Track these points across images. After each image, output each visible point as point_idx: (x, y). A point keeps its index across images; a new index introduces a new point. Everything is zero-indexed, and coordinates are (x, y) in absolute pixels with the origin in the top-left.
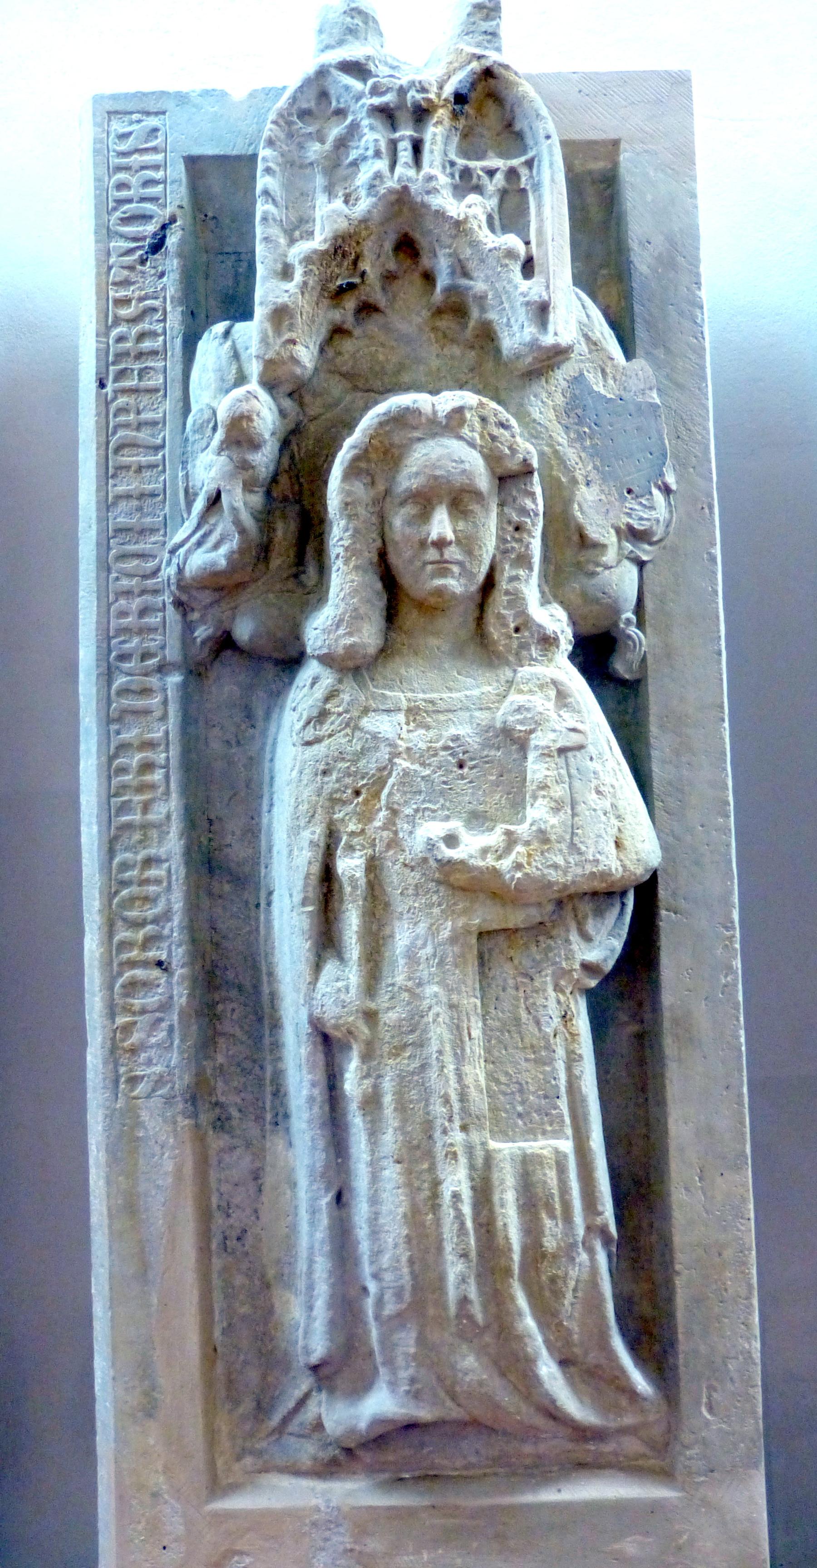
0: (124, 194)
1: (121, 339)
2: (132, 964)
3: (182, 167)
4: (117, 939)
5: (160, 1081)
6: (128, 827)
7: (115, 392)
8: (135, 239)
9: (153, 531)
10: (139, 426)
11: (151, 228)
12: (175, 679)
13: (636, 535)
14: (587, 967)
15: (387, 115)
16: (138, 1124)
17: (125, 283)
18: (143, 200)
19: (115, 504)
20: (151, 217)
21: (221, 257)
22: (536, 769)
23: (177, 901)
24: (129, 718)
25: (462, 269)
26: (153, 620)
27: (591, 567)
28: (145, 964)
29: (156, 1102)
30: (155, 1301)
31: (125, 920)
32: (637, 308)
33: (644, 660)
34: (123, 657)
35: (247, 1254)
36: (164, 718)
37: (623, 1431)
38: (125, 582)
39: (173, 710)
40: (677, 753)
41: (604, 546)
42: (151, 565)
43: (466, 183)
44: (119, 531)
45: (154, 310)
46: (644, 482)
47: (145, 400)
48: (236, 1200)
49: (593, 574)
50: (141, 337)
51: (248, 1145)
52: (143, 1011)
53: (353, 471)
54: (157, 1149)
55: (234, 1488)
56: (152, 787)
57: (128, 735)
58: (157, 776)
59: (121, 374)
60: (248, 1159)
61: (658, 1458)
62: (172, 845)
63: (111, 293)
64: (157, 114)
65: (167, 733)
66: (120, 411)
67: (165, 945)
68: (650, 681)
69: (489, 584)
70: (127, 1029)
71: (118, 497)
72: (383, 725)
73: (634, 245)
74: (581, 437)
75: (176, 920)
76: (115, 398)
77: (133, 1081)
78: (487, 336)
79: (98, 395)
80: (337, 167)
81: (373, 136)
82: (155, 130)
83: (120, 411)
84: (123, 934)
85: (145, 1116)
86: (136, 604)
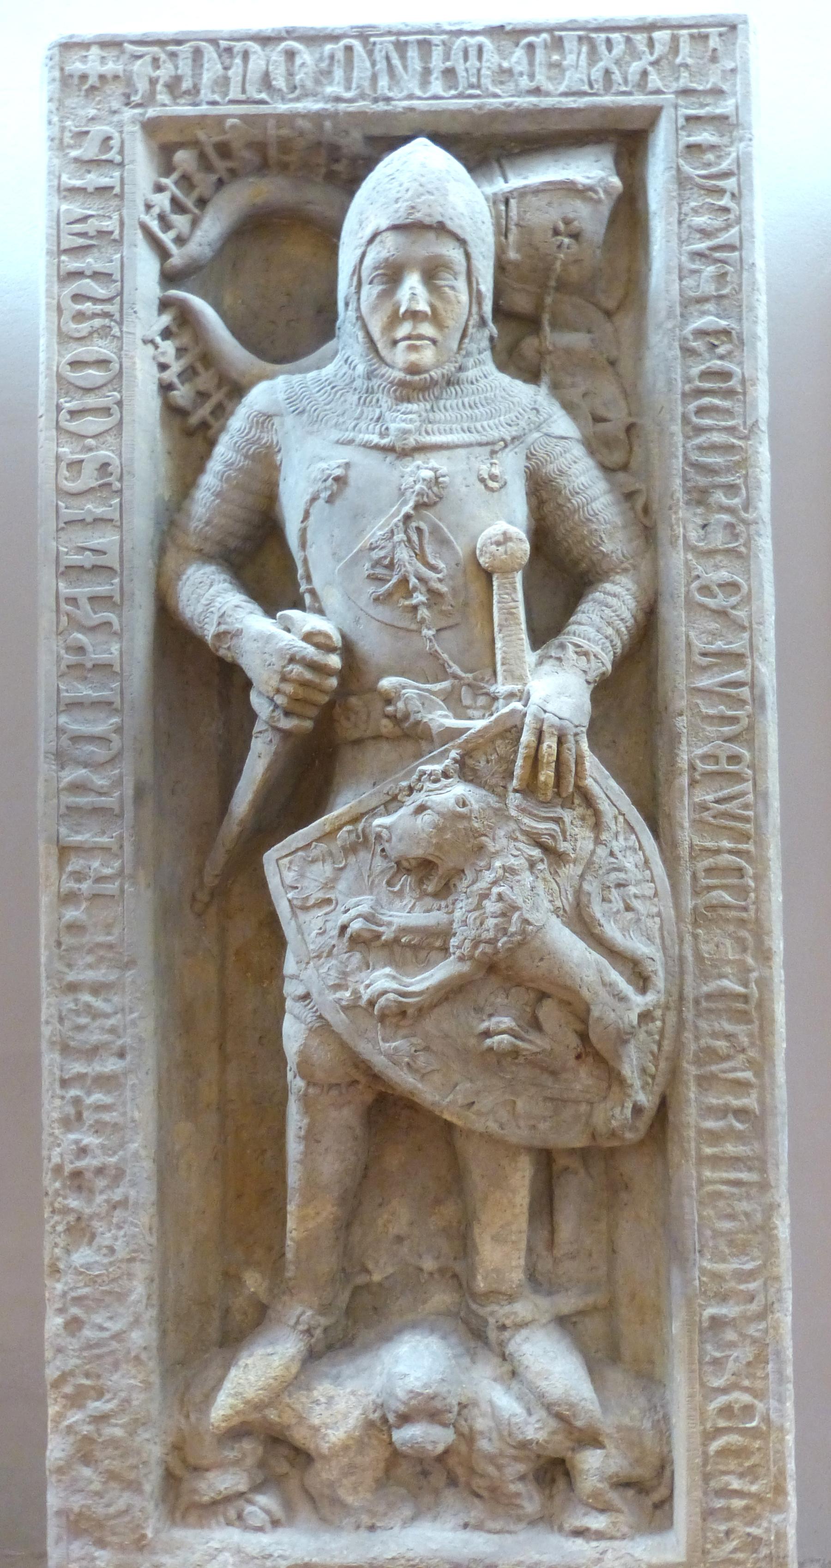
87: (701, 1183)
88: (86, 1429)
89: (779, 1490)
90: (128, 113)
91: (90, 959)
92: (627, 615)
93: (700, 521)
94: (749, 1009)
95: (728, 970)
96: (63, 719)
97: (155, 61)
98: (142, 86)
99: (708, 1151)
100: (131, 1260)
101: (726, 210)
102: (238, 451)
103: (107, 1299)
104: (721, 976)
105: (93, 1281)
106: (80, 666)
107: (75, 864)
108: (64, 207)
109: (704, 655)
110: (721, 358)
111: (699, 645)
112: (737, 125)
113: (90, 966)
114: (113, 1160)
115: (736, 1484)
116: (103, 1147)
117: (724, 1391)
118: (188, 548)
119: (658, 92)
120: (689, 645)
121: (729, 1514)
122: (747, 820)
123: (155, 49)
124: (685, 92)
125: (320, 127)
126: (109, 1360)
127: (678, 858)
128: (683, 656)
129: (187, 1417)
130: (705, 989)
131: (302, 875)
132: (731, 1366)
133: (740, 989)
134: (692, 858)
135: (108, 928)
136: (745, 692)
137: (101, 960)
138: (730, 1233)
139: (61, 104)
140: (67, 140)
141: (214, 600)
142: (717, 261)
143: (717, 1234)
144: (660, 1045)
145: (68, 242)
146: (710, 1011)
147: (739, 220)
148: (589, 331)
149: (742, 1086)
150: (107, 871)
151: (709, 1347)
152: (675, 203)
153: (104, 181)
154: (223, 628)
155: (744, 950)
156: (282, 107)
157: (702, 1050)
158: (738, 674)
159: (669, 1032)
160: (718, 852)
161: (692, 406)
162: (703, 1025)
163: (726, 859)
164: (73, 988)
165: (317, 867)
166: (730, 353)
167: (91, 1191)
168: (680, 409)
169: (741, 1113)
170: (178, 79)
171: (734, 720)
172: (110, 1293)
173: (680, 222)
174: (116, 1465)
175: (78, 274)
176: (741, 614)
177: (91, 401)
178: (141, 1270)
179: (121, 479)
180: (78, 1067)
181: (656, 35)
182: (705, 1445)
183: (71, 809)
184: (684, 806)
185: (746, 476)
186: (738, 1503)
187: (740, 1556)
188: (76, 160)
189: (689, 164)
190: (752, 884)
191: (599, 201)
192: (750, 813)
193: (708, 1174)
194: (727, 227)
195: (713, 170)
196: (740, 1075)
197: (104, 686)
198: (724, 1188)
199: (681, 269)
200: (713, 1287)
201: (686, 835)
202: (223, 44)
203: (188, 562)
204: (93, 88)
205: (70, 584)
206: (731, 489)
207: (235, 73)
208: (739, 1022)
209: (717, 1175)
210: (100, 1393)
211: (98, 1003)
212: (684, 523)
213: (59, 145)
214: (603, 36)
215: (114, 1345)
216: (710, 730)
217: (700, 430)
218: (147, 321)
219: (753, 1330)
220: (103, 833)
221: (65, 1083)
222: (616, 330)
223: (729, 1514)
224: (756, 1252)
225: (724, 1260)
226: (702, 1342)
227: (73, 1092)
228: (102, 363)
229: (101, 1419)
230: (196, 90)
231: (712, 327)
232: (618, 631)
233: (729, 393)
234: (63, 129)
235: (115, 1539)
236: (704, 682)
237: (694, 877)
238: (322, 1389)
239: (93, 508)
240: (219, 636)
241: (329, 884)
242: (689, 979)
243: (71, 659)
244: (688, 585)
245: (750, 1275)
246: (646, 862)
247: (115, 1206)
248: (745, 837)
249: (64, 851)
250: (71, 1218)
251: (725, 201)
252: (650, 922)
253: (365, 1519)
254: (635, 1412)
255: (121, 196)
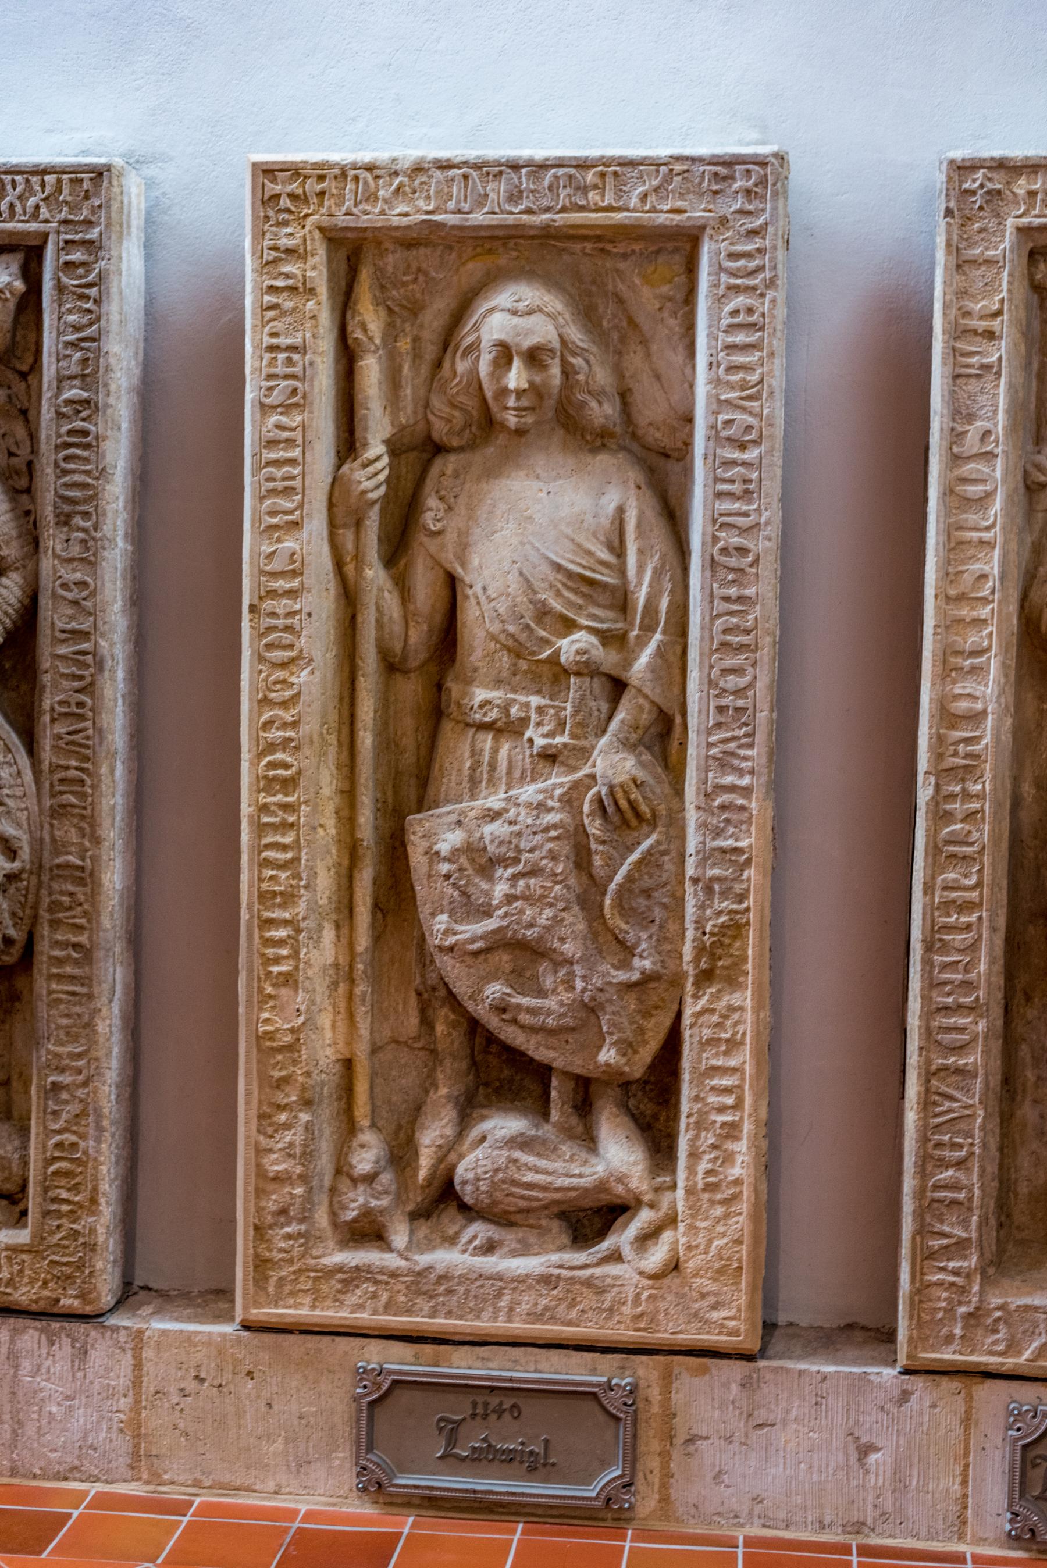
87: (50, 992)
89: (94, 1201)
92: (13, 600)
93: (64, 537)
94: (86, 877)
95: (73, 849)
99: (55, 971)
101: (89, 311)
104: (69, 853)
109: (64, 632)
110: (83, 420)
111: (60, 625)
112: (100, 248)
115: (64, 1195)
117: (59, 1132)
119: (47, 221)
120: (53, 624)
121: (59, 1214)
122: (88, 747)
124: (65, 222)
127: (41, 771)
128: (49, 632)
130: (57, 861)
132: (64, 1116)
133: (79, 863)
134: (51, 772)
136: (89, 659)
138: (67, 1027)
142: (82, 349)
143: (58, 1027)
144: (25, 896)
146: (59, 876)
147: (98, 319)
148: (9, 388)
149: (80, 928)
151: (50, 1103)
152: (55, 305)
155: (84, 836)
157: (53, 902)
158: (85, 646)
159: (32, 890)
160: (67, 768)
161: (61, 455)
162: (55, 886)
163: (73, 773)
166: (90, 416)
168: (53, 457)
169: (76, 946)
171: (81, 678)
173: (60, 319)
176: (88, 604)
181: (47, 178)
182: (46, 1168)
184: (48, 733)
185: (97, 506)
186: (65, 1208)
187: (65, 1242)
189: (66, 276)
190: (90, 791)
191: (6, 300)
192: (90, 743)
193: (54, 986)
194: (91, 324)
195: (83, 281)
196: (77, 921)
198: (64, 996)
199: (58, 355)
200: (55, 1062)
201: (47, 755)
206: (86, 515)
208: (78, 885)
209: (60, 987)
212: (53, 540)
214: (9, 177)
216: (65, 683)
217: (66, 472)
219: (81, 1093)
222: (28, 387)
223: (59, 1214)
224: (83, 1041)
225: (62, 1045)
226: (46, 1099)
231: (77, 398)
232: (6, 613)
233: (87, 446)
236: (63, 650)
237: (52, 785)
242: (46, 854)
244: (54, 582)
245: (79, 1056)
246: (19, 773)
248: (87, 759)
251: (89, 305)
252: (19, 814)
254: (9, 1148)
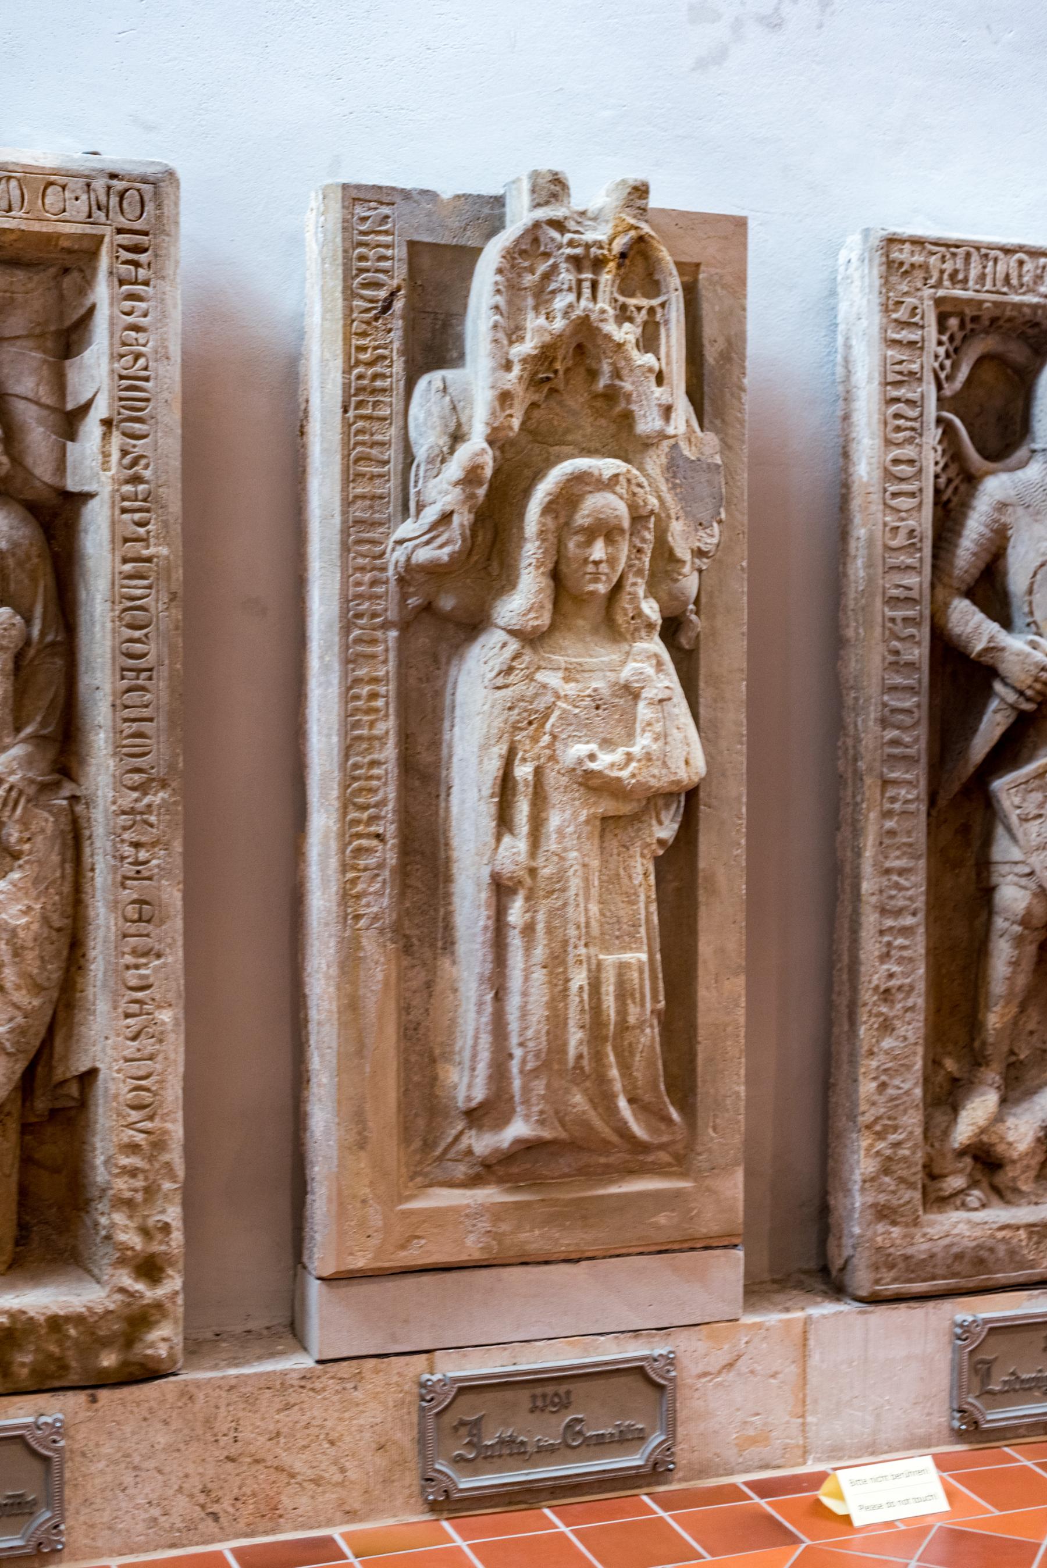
0: (363, 264)
1: (360, 377)
2: (359, 836)
3: (405, 249)
4: (349, 817)
5: (376, 918)
6: (359, 738)
7: (356, 417)
8: (371, 301)
9: (381, 524)
10: (373, 445)
11: (383, 294)
12: (393, 634)
13: (700, 553)
14: (661, 842)
15: (577, 262)
16: (359, 947)
17: (364, 334)
18: (377, 271)
19: (353, 502)
20: (383, 285)
21: (424, 315)
22: (644, 711)
23: (391, 792)
24: (361, 660)
25: (617, 374)
26: (380, 590)
27: (675, 575)
28: (368, 836)
29: (372, 932)
30: (368, 1069)
31: (354, 804)
32: (706, 389)
33: (698, 636)
34: (359, 616)
35: (419, 1040)
36: (385, 662)
37: (661, 1147)
38: (360, 561)
39: (392, 655)
40: (715, 701)
41: (684, 562)
42: (378, 549)
43: (624, 315)
44: (358, 522)
45: (384, 357)
46: (709, 518)
47: (376, 426)
48: (414, 1003)
49: (677, 580)
50: (375, 377)
51: (424, 964)
52: (366, 869)
53: (548, 509)
54: (372, 965)
55: (409, 1198)
56: (376, 710)
57: (361, 672)
58: (380, 703)
59: (360, 404)
60: (423, 974)
61: (681, 1162)
62: (389, 752)
63: (354, 342)
64: (388, 204)
65: (387, 672)
66: (359, 432)
67: (382, 822)
68: (702, 651)
69: (618, 588)
70: (354, 881)
71: (356, 497)
72: (552, 679)
73: (706, 342)
74: (674, 486)
75: (391, 806)
76: (354, 423)
77: (357, 917)
78: (627, 419)
79: (343, 418)
80: (542, 295)
81: (566, 276)
82: (387, 217)
83: (359, 432)
84: (353, 815)
85: (365, 942)
86: (368, 577)
88: (888, 1152)
90: (927, 292)
91: (898, 853)
96: (886, 698)
97: (943, 259)
98: (935, 275)
100: (916, 1044)
102: (987, 526)
103: (902, 1069)
105: (895, 1058)
106: (896, 663)
107: (891, 792)
108: (890, 353)
113: (898, 858)
114: (908, 981)
116: (902, 972)
118: (951, 587)
123: (943, 249)
125: (1035, 314)
126: (902, 1108)
129: (932, 1146)
131: (1024, 800)
135: (909, 833)
137: (904, 853)
139: (887, 282)
140: (891, 307)
141: (970, 622)
145: (891, 377)
150: (910, 797)
153: (913, 337)
154: (992, 645)
156: (1017, 299)
164: (888, 871)
165: (1034, 795)
167: (893, 1002)
170: (956, 272)
172: (902, 1065)
174: (904, 1173)
175: (897, 400)
177: (905, 487)
178: (920, 1050)
179: (921, 540)
180: (889, 923)
183: (891, 756)
188: (896, 320)
197: (909, 677)
202: (983, 251)
203: (952, 596)
204: (906, 272)
205: (891, 609)
207: (988, 270)
210: (895, 1129)
211: (902, 881)
213: (886, 309)
215: (905, 1098)
218: (933, 435)
220: (907, 772)
221: (882, 933)
227: (886, 939)
228: (911, 462)
229: (897, 1145)
230: (966, 280)
234: (888, 298)
235: (903, 1219)
238: (1011, 1121)
239: (904, 559)
240: (987, 650)
241: (1041, 806)
243: (891, 658)
247: (907, 1010)
249: (886, 783)
250: (881, 1019)
253: (1034, 1199)
255: (922, 348)
